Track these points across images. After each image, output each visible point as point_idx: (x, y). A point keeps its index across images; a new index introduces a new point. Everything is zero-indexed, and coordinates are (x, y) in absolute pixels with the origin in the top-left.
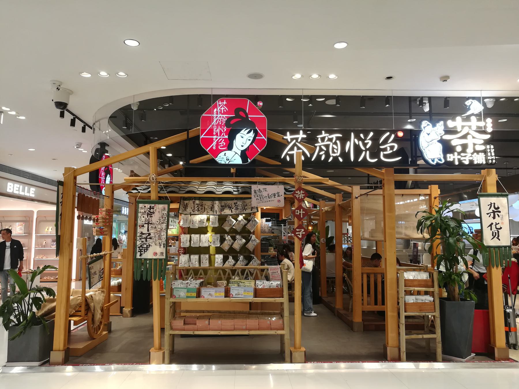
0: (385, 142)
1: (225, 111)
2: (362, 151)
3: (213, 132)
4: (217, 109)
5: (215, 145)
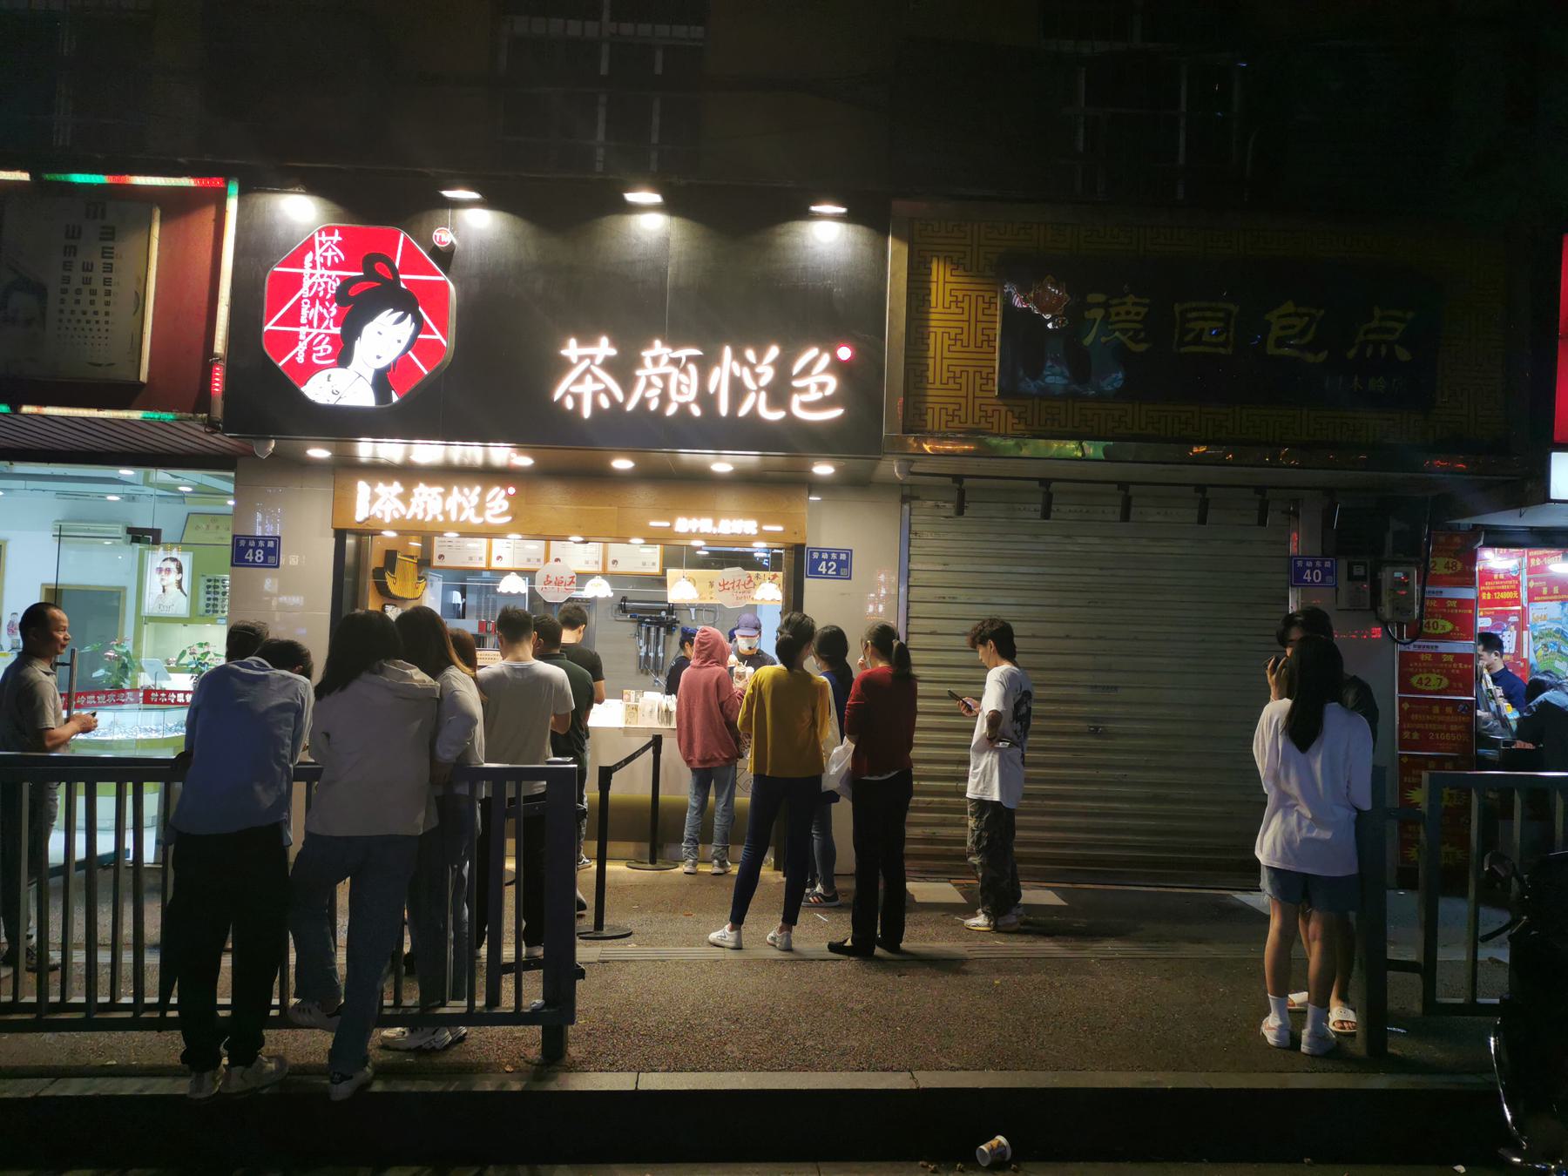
1: (337, 260)
3: (299, 316)
4: (314, 256)
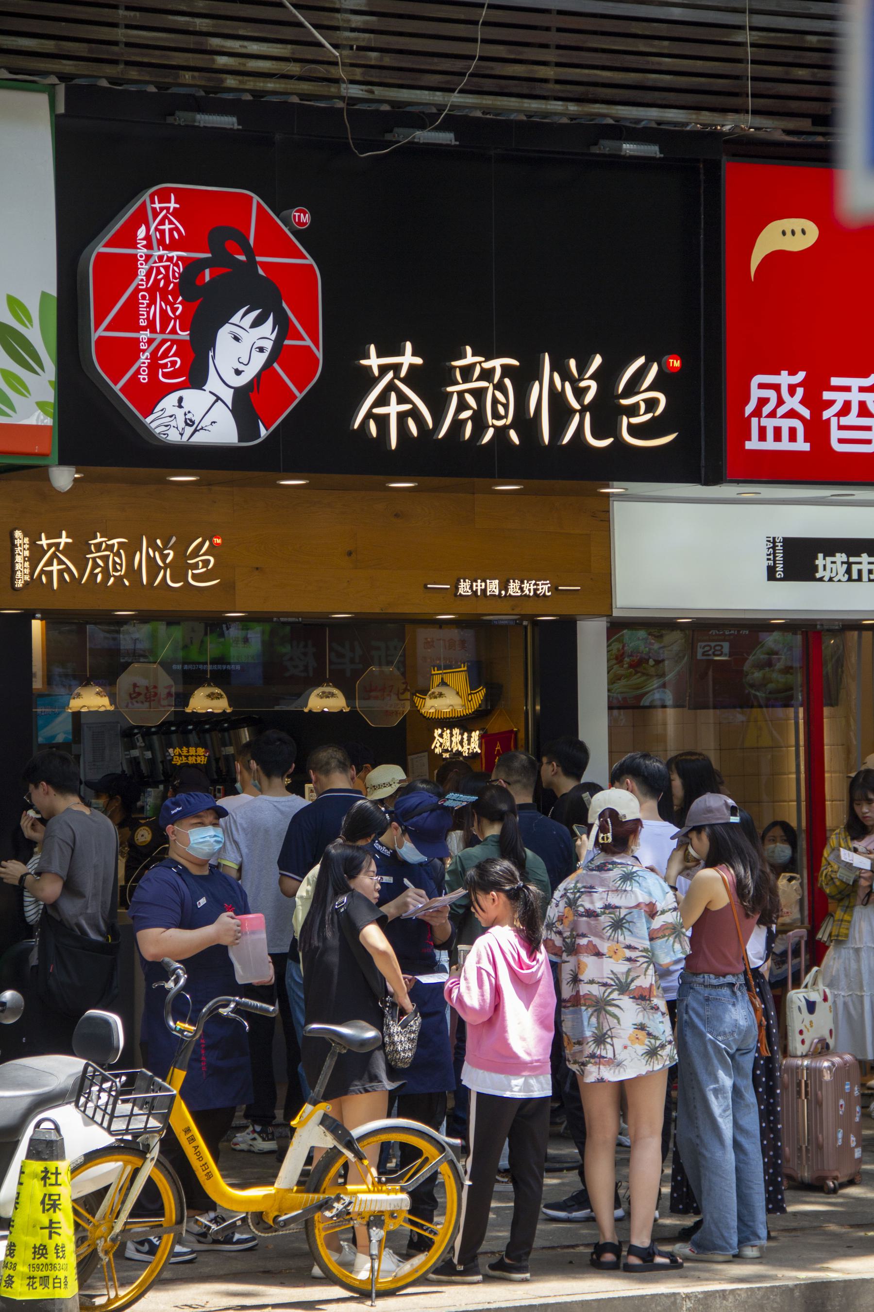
0: (632, 388)
2: (574, 411)
3: (137, 315)
5: (144, 367)
